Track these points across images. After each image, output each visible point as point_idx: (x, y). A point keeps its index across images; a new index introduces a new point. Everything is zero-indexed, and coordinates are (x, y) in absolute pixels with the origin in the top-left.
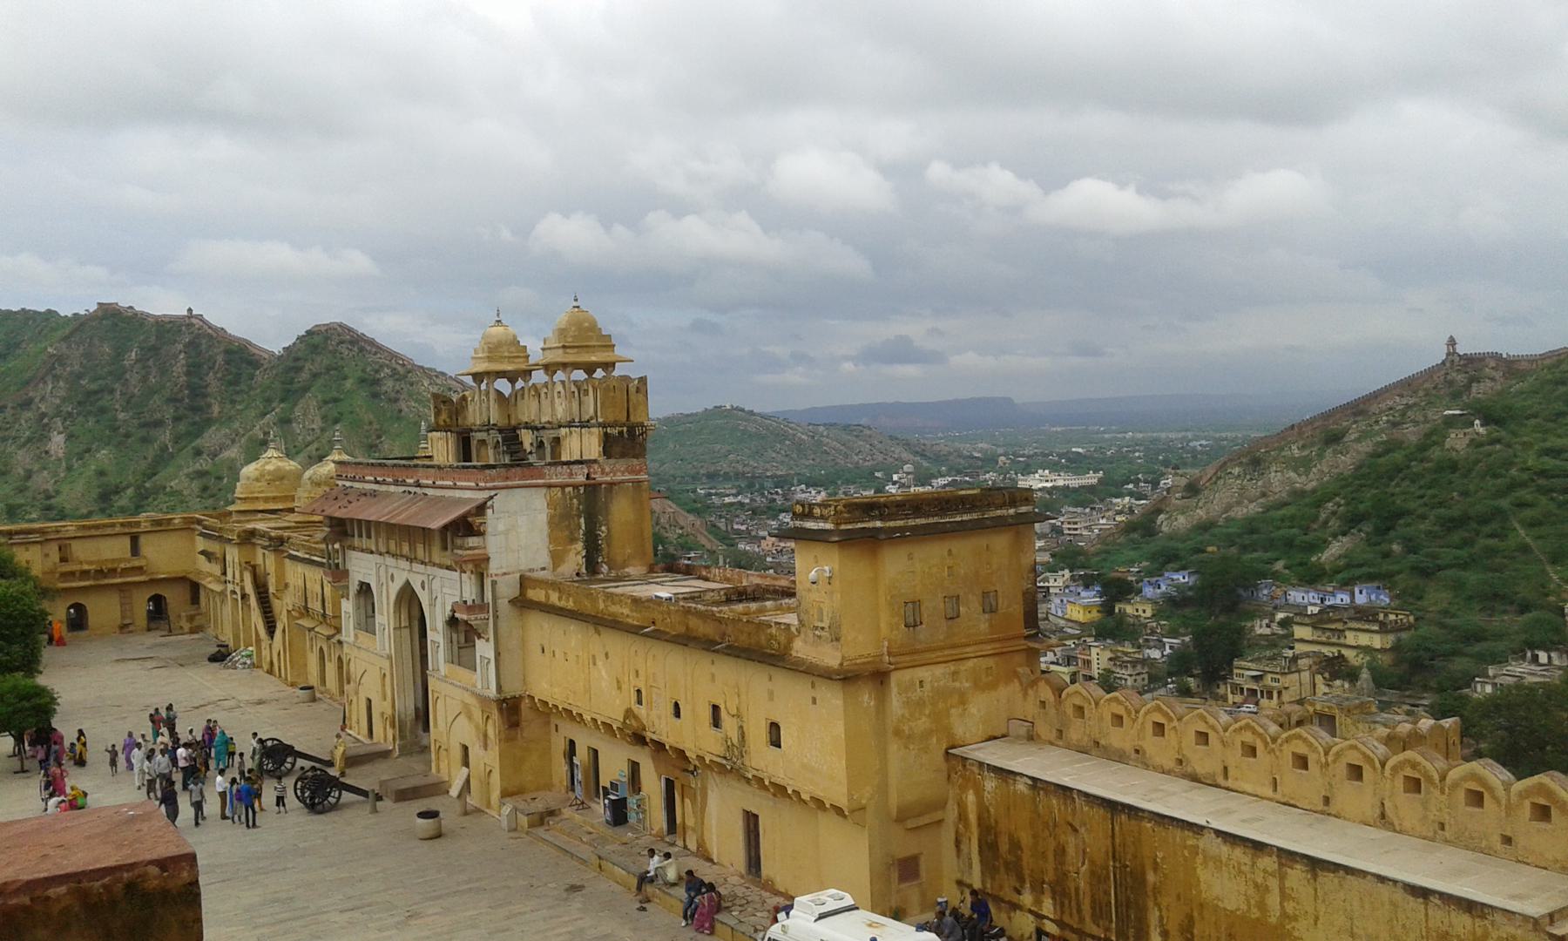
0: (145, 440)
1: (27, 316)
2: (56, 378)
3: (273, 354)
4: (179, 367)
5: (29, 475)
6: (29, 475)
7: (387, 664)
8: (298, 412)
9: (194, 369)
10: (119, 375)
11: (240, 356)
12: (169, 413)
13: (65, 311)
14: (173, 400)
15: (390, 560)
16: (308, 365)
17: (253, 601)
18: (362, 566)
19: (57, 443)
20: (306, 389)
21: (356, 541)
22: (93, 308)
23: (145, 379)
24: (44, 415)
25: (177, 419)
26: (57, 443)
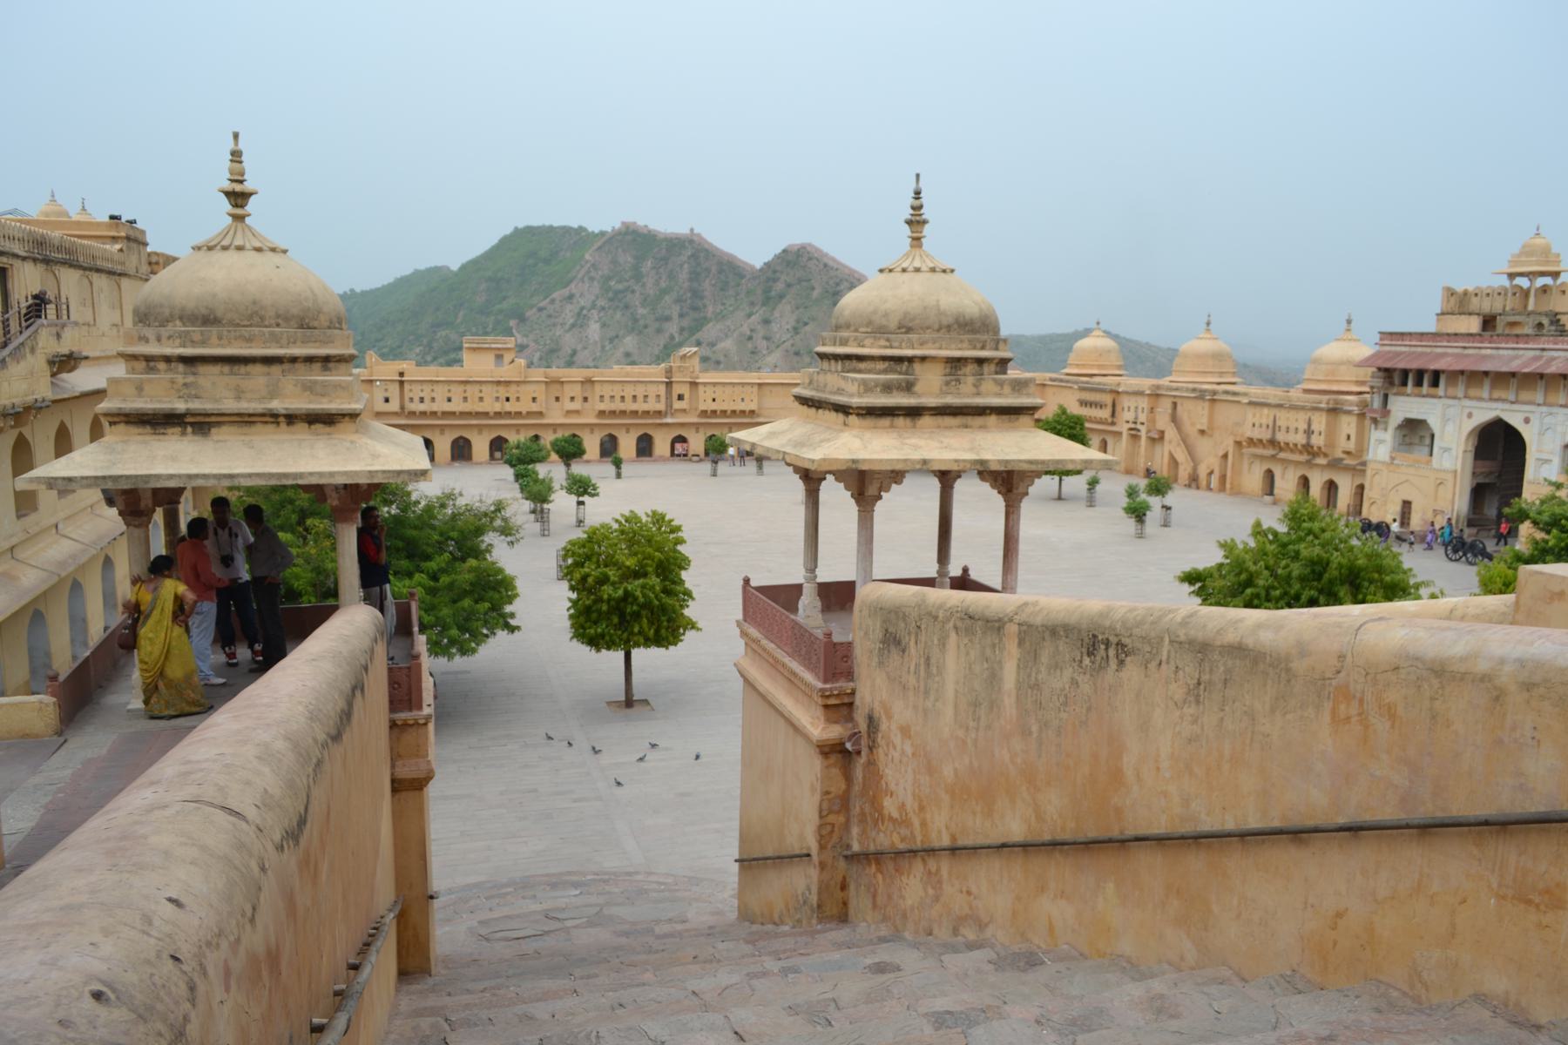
0: (659, 331)
1: (566, 230)
2: (592, 279)
3: (752, 267)
4: (683, 275)
5: (574, 353)
6: (574, 353)
7: (1450, 477)
8: (777, 314)
9: (695, 276)
10: (638, 277)
11: (729, 269)
12: (675, 311)
13: (594, 227)
14: (678, 301)
15: (1467, 402)
16: (783, 277)
17: (1171, 433)
18: (1405, 406)
19: (594, 330)
20: (781, 297)
21: (1410, 388)
22: (618, 226)
23: (657, 283)
24: (582, 308)
25: (681, 316)
26: (594, 330)
